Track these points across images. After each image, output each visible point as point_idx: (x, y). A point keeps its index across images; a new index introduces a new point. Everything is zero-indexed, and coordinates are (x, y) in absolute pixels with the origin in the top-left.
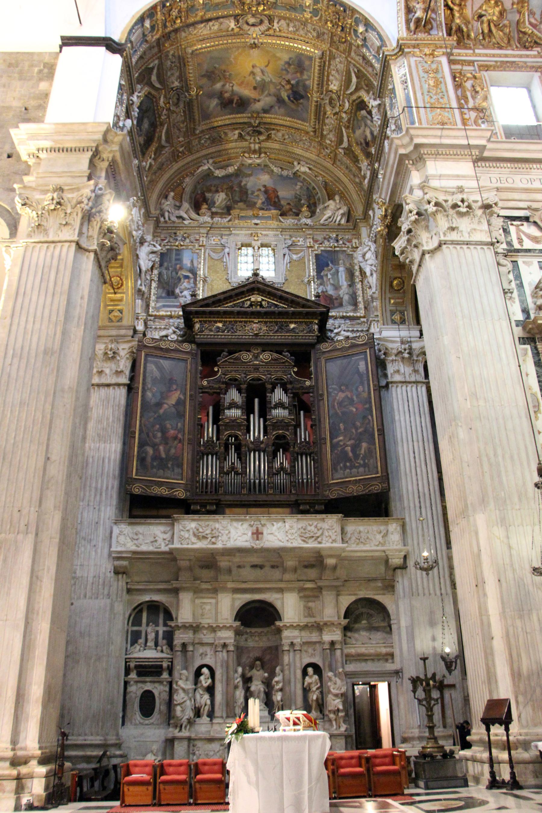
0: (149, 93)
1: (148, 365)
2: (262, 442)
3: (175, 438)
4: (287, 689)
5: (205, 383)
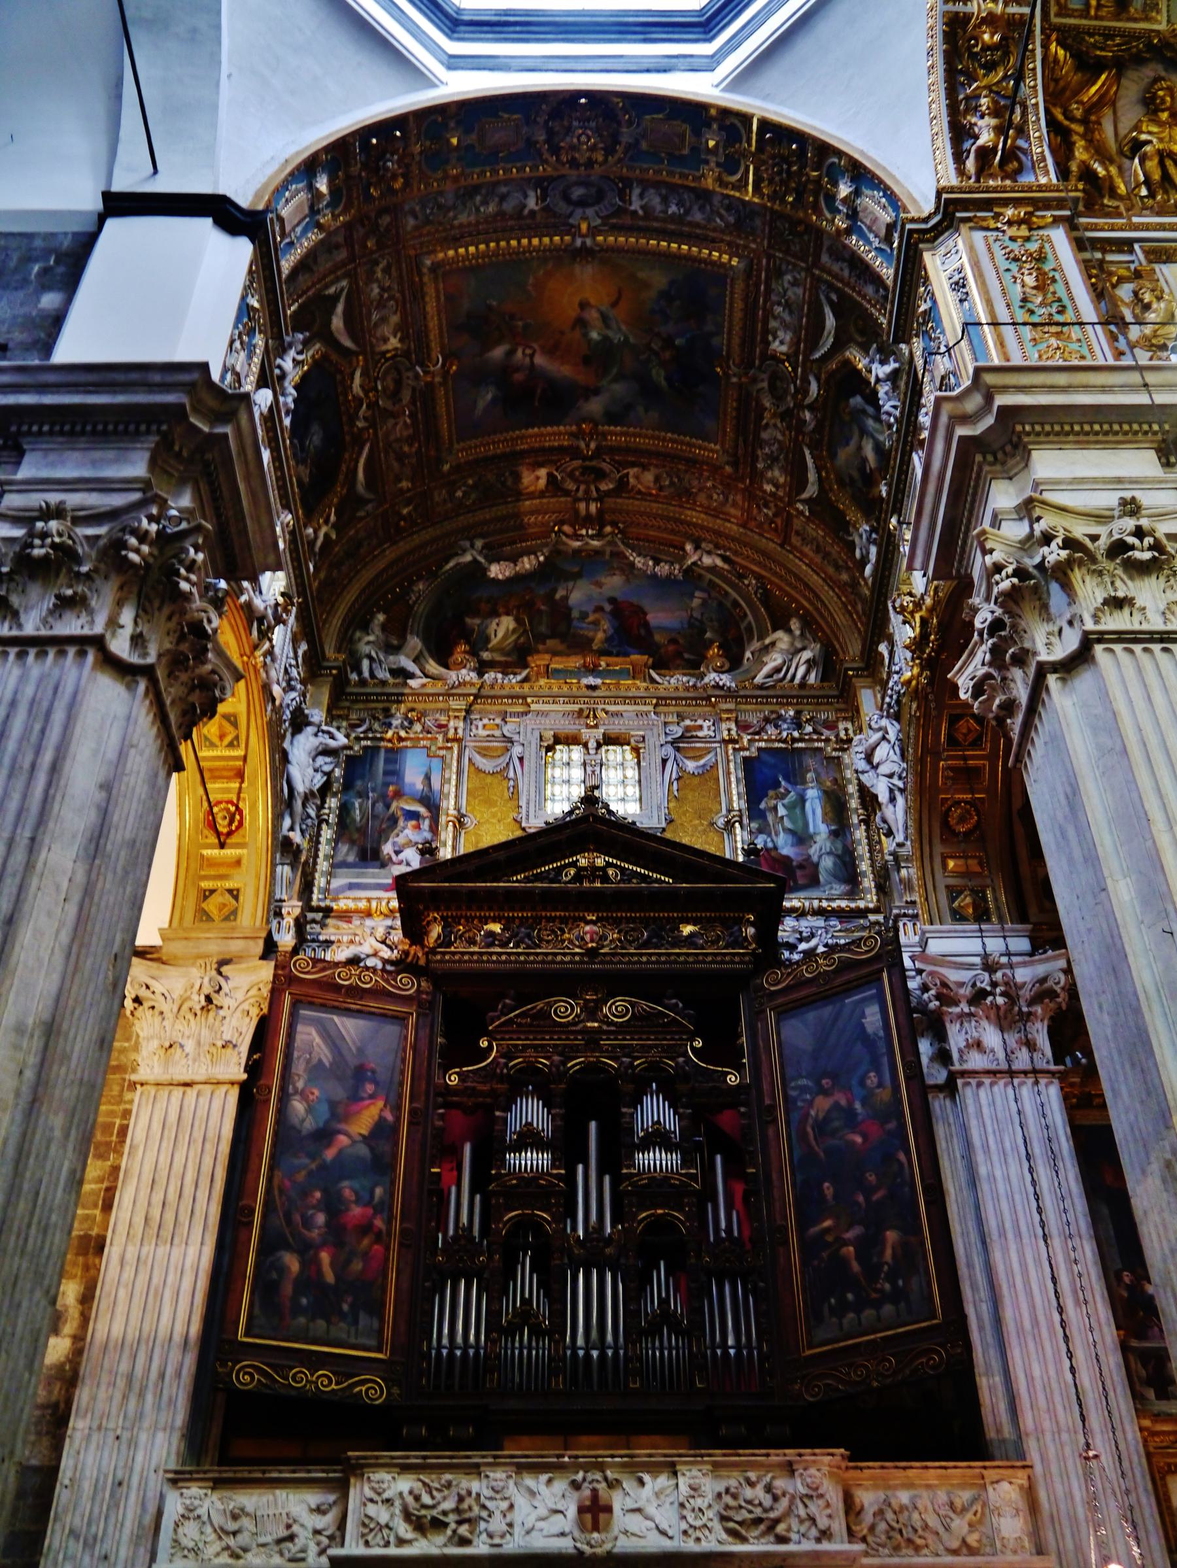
0: (325, 357)
2: (609, 1241)
3: (366, 1228)
5: (453, 1080)
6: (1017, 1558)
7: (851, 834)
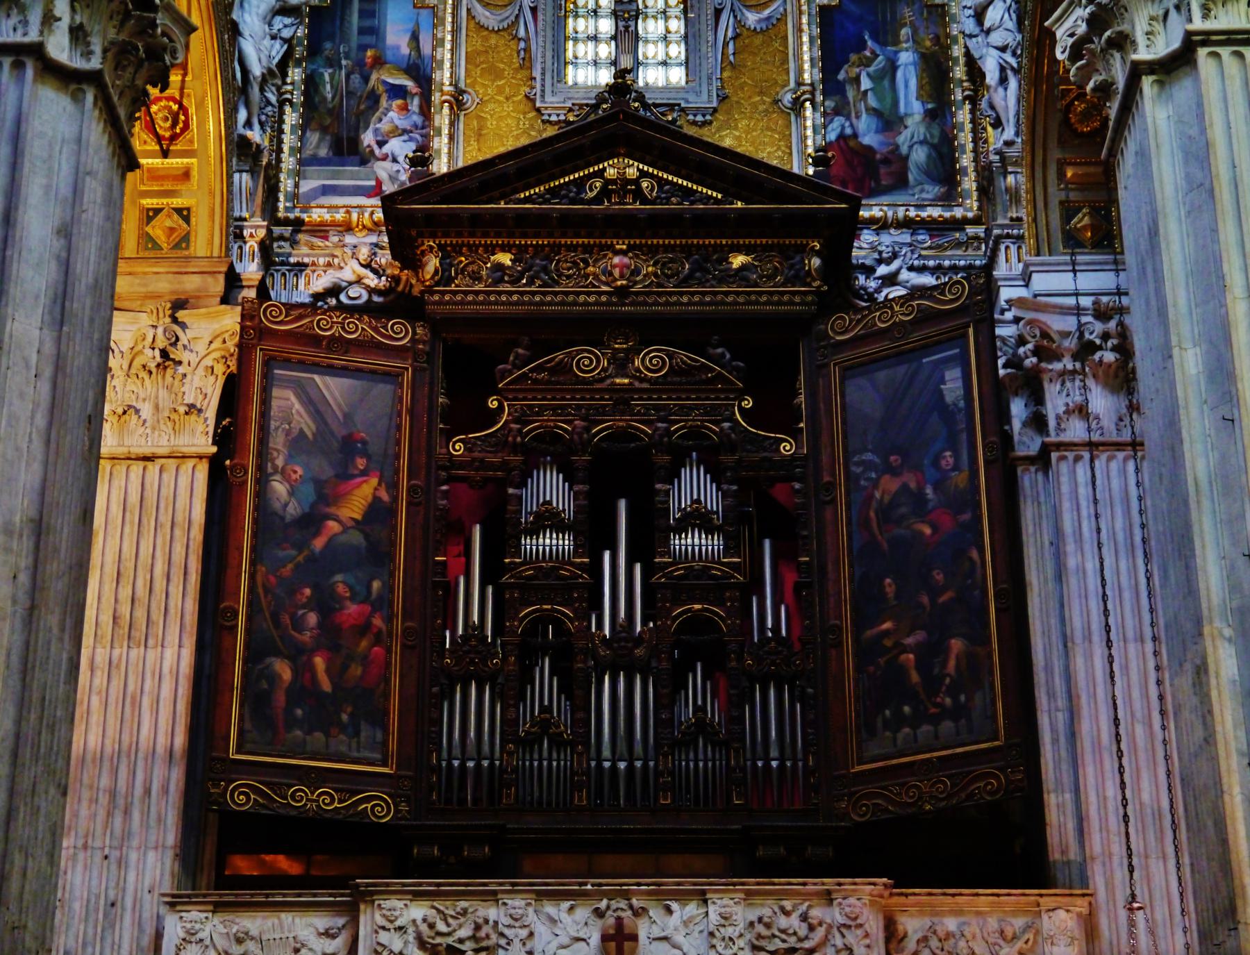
1: (276, 392)
2: (639, 640)
3: (364, 628)
5: (458, 449)
7: (953, 115)
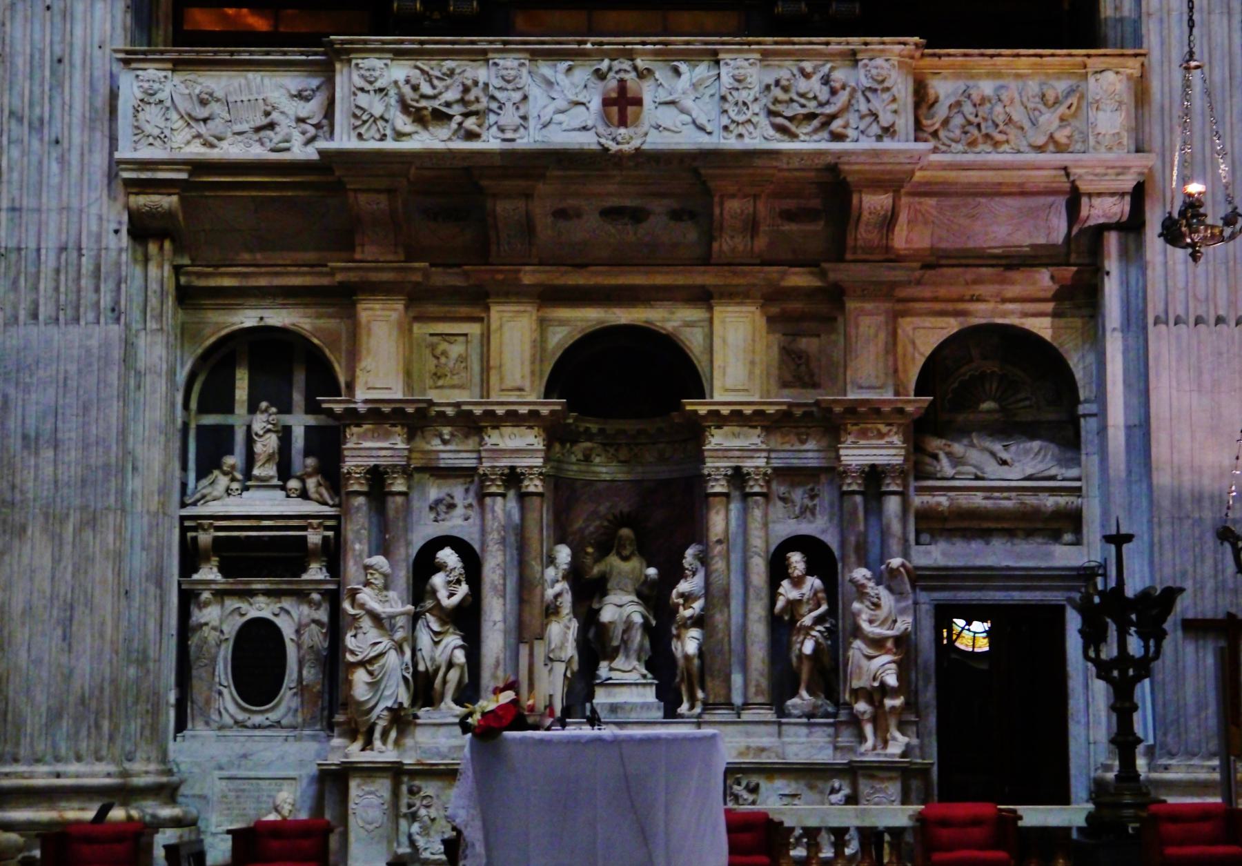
4: (719, 618)
6: (1111, 156)
